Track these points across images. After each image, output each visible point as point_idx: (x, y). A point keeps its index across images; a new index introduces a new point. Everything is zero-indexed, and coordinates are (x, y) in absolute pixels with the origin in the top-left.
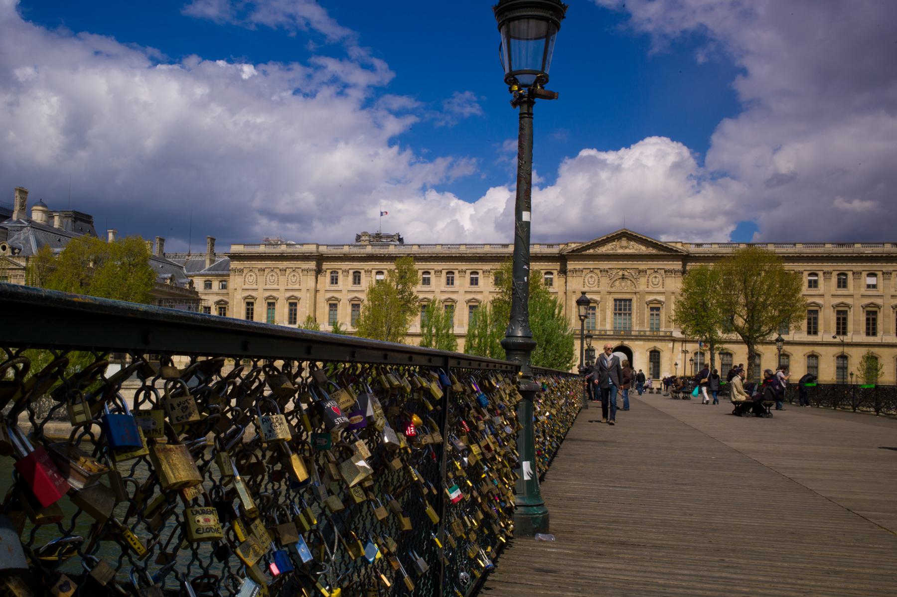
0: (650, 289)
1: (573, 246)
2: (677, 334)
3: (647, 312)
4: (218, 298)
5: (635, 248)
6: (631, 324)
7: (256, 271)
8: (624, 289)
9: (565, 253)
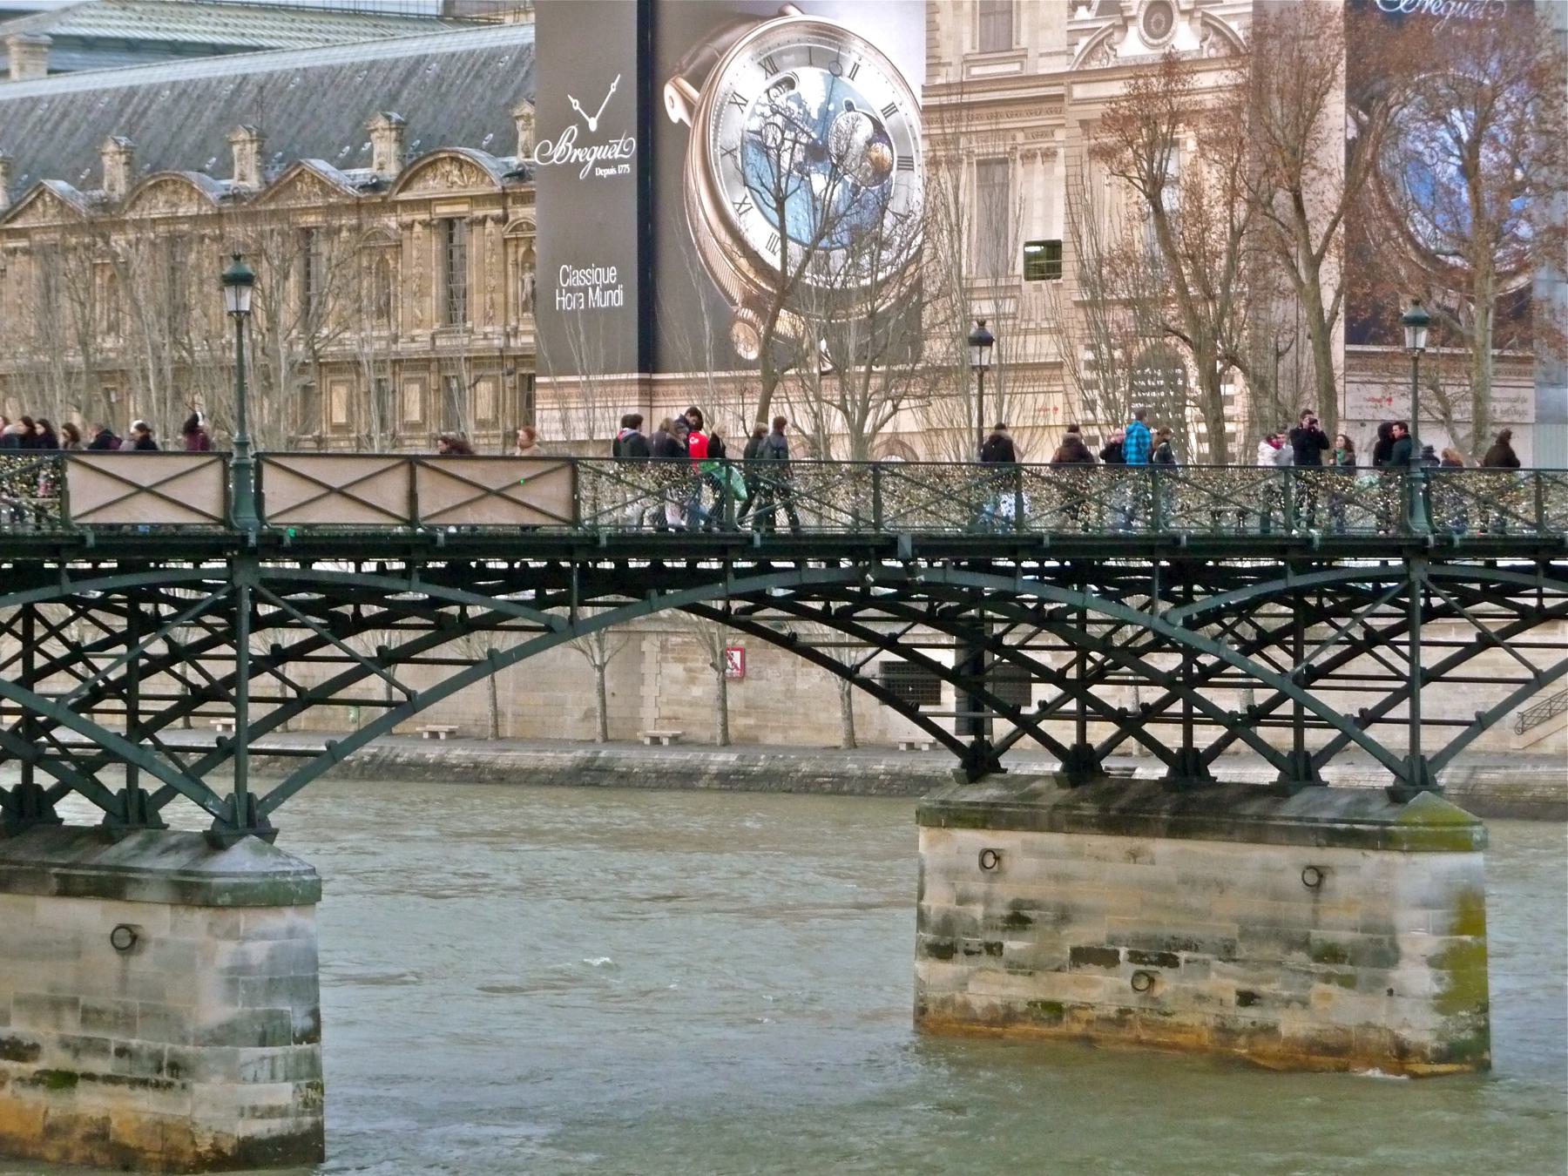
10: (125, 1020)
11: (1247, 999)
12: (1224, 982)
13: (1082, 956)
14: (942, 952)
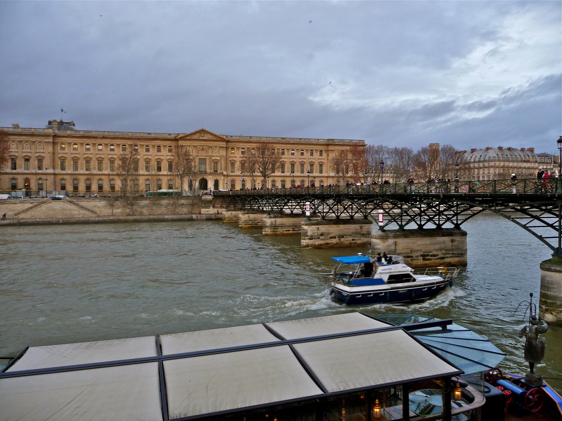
0: (213, 155)
1: (181, 135)
2: (225, 173)
3: (213, 164)
5: (207, 137)
6: (206, 169)
7: (17, 142)
8: (203, 155)
9: (178, 138)
10: (430, 252)
11: (353, 240)
12: (350, 239)
13: (331, 238)
14: (311, 239)
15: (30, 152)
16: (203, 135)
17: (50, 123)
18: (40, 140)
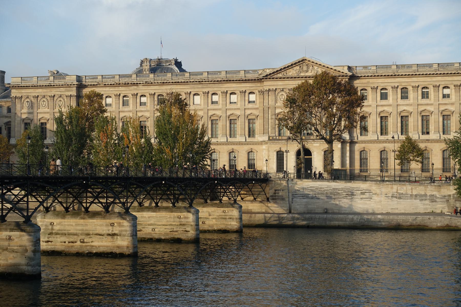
1: (268, 72)
4: (6, 120)
15: (48, 113)
16: (305, 68)
17: (142, 62)
18: (60, 93)
